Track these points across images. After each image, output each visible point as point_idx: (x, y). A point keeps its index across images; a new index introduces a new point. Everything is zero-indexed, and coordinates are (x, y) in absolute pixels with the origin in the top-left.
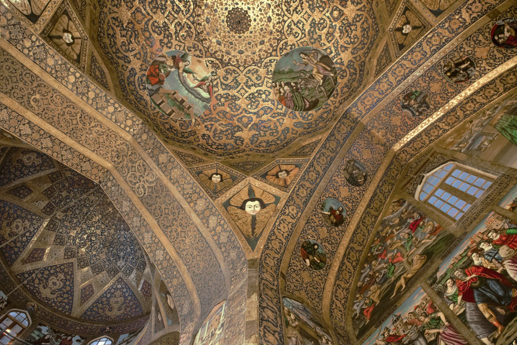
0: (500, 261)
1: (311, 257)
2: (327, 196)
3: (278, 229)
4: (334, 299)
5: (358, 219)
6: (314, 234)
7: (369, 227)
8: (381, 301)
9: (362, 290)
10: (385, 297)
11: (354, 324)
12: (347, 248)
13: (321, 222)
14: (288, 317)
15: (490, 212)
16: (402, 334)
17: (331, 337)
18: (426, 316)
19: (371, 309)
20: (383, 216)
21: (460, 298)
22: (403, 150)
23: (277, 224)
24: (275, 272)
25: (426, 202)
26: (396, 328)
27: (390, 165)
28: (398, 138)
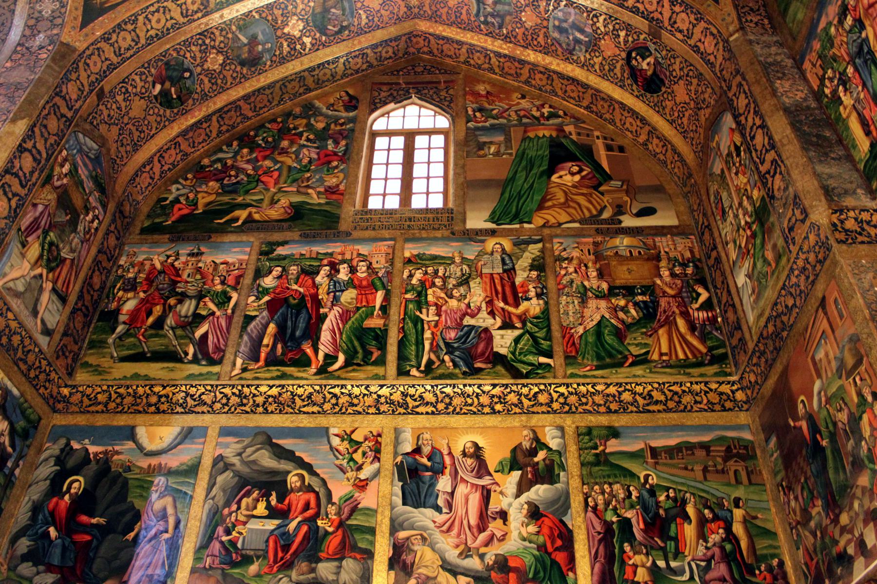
0: (336, 300)
1: (167, 84)
2: (264, 15)
3: (146, 17)
4: (156, 159)
5: (281, 76)
6: (198, 55)
7: (286, 96)
8: (204, 212)
9: (201, 173)
10: (213, 212)
11: (153, 210)
12: (231, 103)
13: (222, 45)
14: (57, 169)
15: (391, 239)
16: (185, 276)
17: (105, 213)
18: (223, 283)
19: (186, 211)
20: (318, 98)
21: (267, 298)
22: (426, 36)
23: (152, 9)
24: (91, 84)
25: (374, 135)
26: (186, 263)
27: (391, 40)
28: (434, 17)
